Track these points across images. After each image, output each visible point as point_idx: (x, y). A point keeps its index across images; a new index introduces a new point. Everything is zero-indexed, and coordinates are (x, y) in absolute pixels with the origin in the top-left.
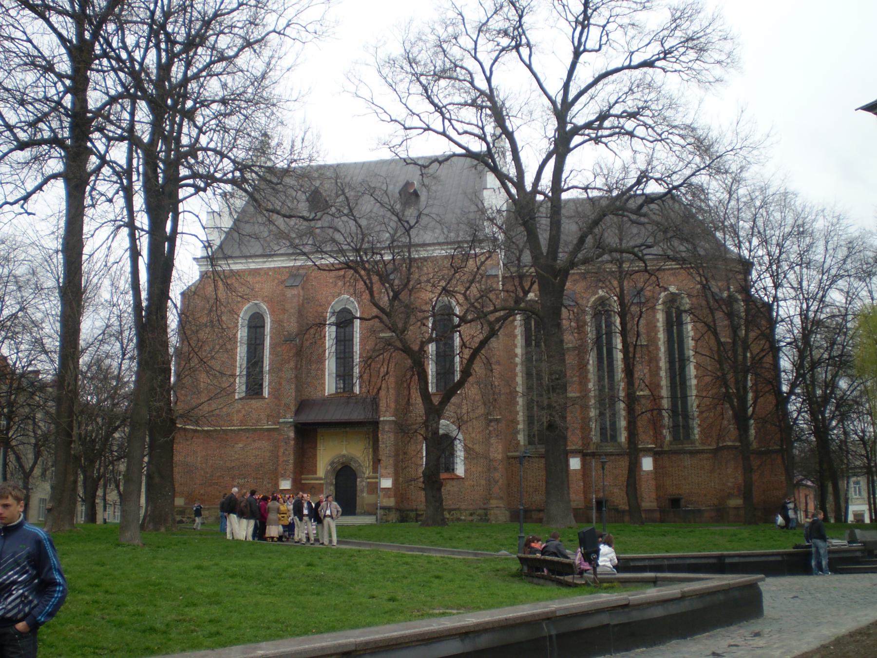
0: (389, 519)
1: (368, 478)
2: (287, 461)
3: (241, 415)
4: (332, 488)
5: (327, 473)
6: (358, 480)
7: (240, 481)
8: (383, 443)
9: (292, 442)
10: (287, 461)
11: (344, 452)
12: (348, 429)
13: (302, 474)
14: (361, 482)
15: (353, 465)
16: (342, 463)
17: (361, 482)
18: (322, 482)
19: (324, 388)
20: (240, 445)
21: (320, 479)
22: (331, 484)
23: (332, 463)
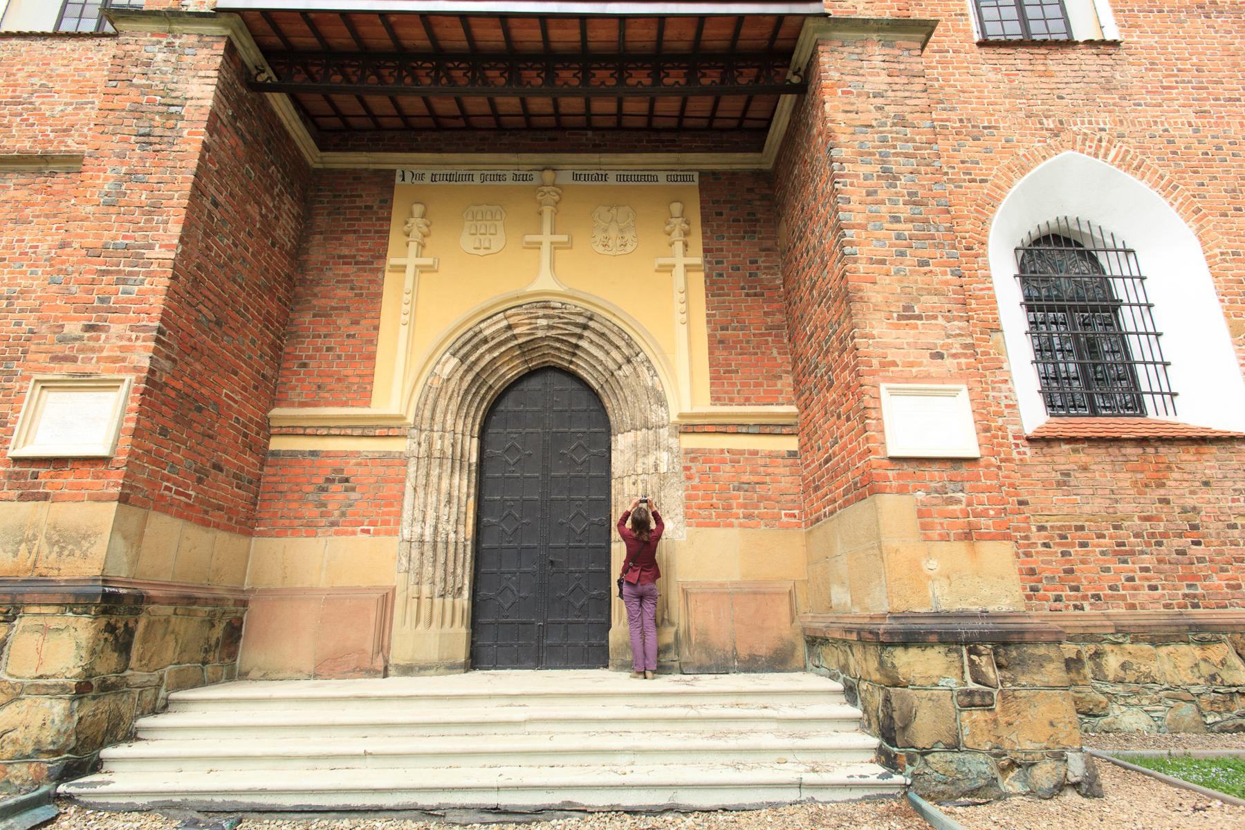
0: (1024, 742)
1: (688, 429)
2: (133, 253)
4: (463, 486)
5: (431, 399)
6: (622, 445)
8: (863, 154)
10: (133, 253)
11: (544, 282)
12: (565, 177)
13: (274, 403)
14: (640, 451)
16: (527, 348)
17: (640, 451)
21: (387, 428)
22: (458, 461)
23: (469, 345)
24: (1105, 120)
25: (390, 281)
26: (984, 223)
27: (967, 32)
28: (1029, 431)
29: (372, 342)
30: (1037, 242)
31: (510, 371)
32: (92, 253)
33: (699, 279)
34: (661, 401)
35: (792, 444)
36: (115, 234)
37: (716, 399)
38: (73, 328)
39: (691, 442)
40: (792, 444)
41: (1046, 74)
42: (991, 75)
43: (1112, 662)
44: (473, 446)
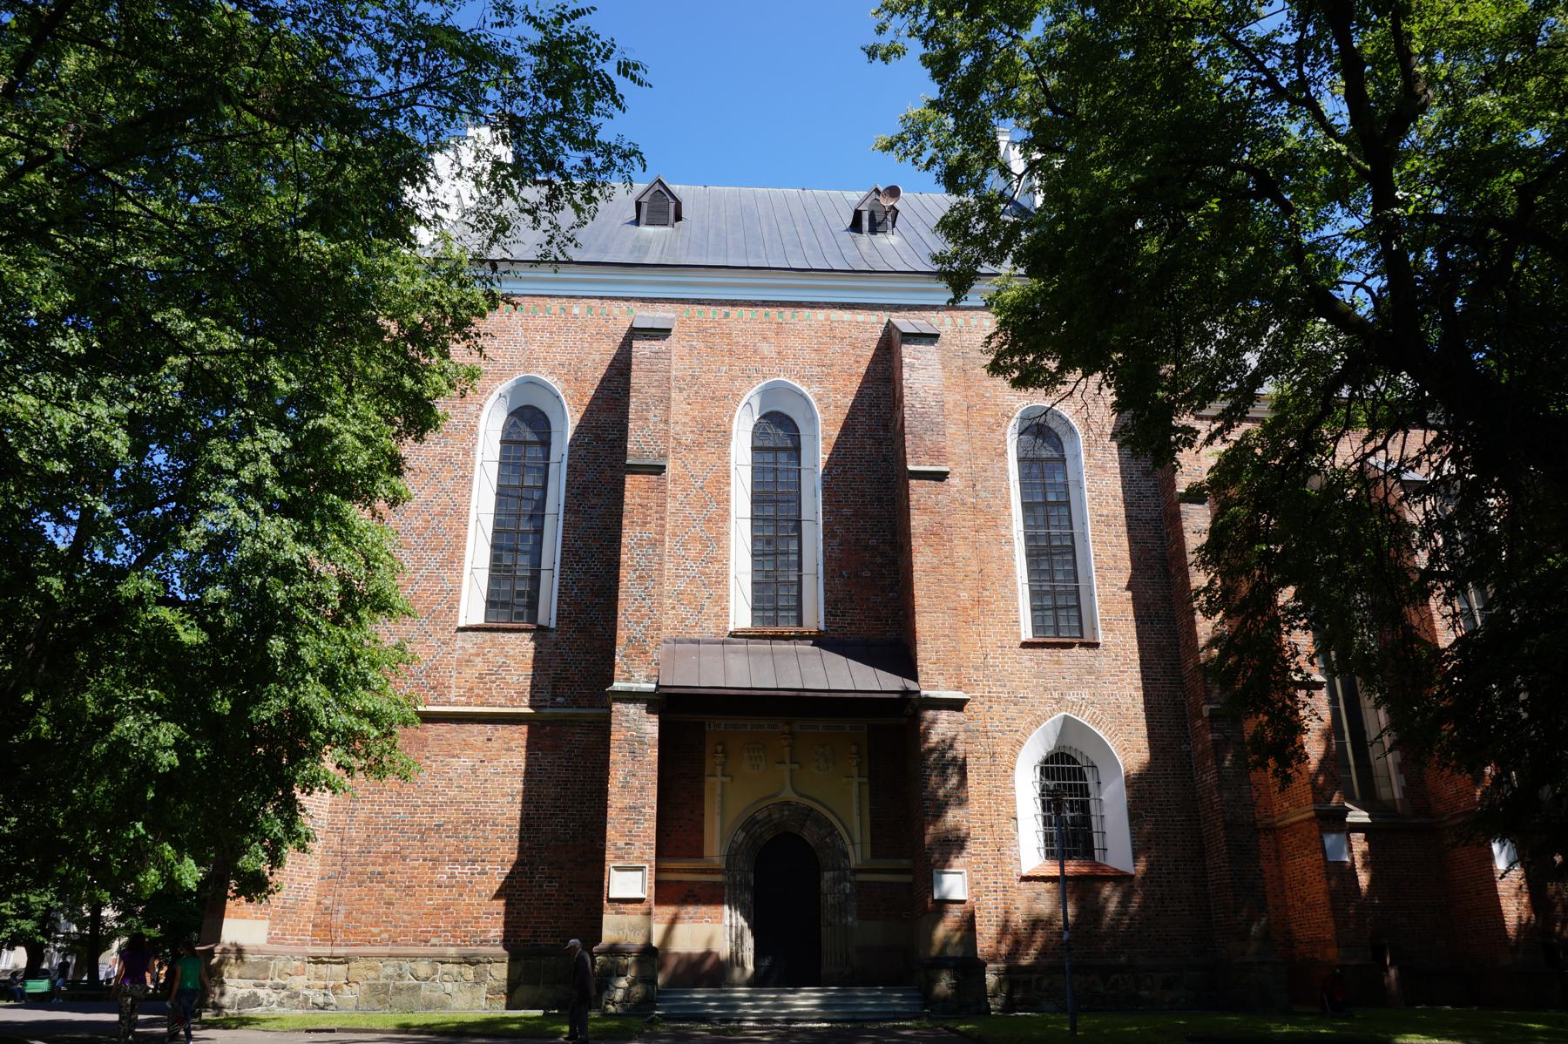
3: (470, 673)
5: (731, 856)
6: (828, 875)
7: (458, 869)
9: (653, 754)
11: (788, 794)
15: (810, 834)
17: (837, 881)
18: (719, 878)
19: (725, 609)
20: (464, 763)
23: (749, 825)
24: (1086, 693)
25: (707, 787)
26: (1015, 755)
27: (1018, 635)
28: (1025, 873)
29: (701, 823)
30: (1046, 762)
31: (768, 837)
32: (621, 810)
33: (866, 789)
34: (846, 856)
35: (908, 878)
36: (628, 801)
37: (873, 856)
38: (621, 844)
39: (861, 877)
40: (908, 878)
41: (1058, 662)
42: (1028, 664)
43: (1045, 983)
44: (751, 876)
